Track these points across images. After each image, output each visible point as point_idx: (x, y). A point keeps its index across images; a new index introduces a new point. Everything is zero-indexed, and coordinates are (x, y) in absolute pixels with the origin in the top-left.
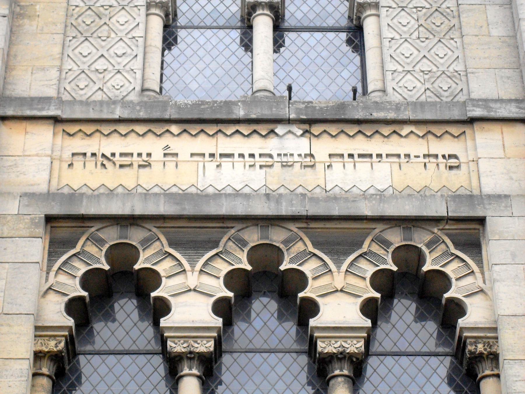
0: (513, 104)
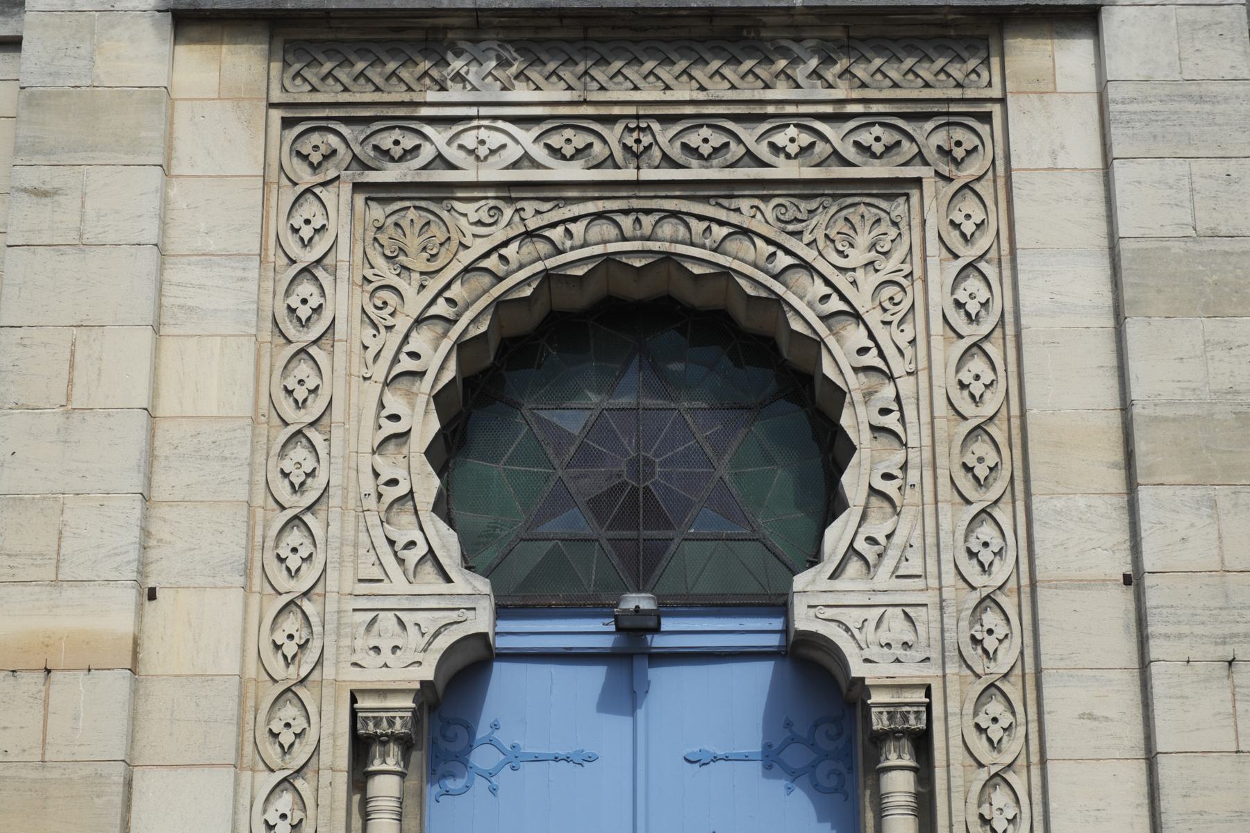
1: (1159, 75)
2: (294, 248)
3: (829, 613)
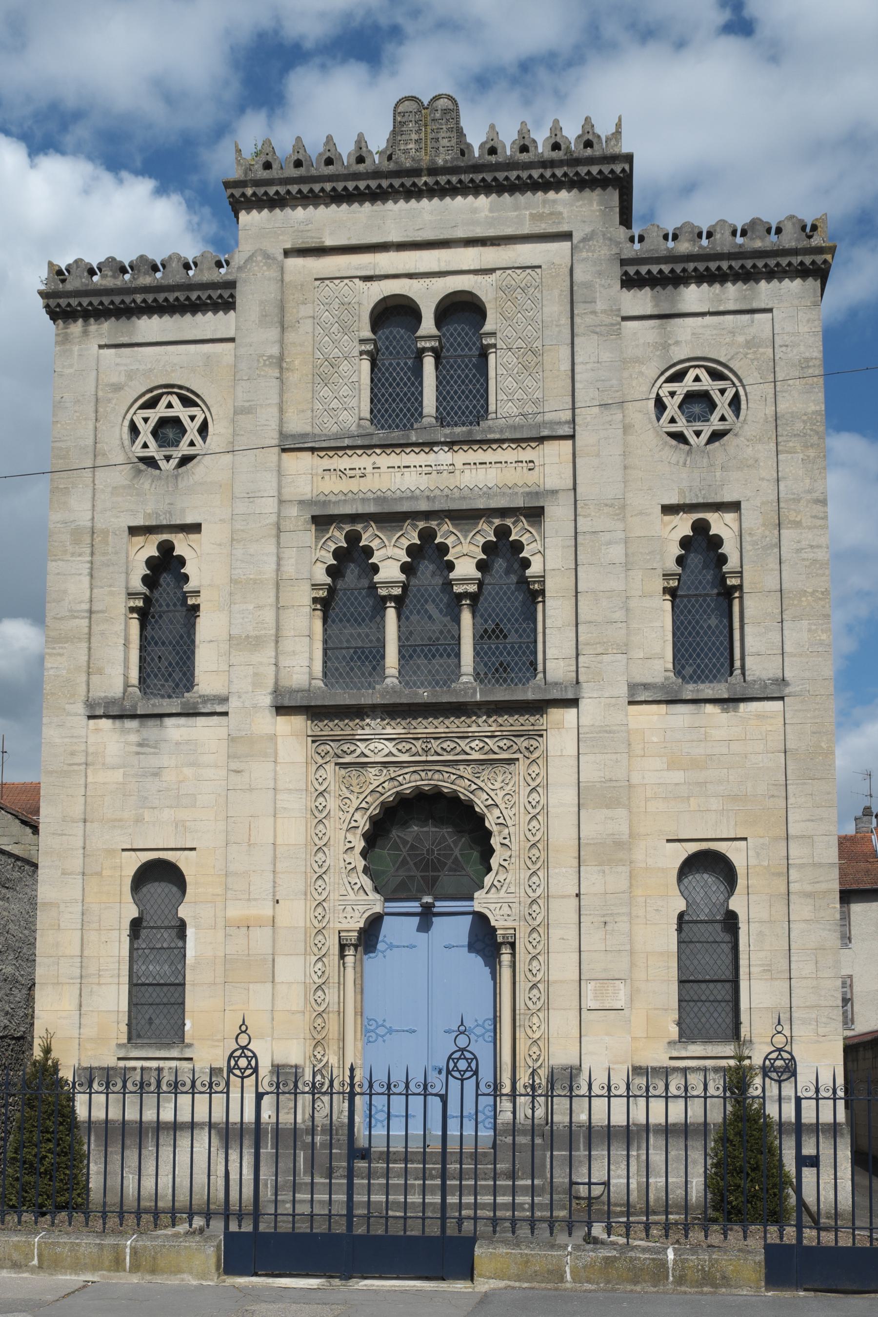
0: (567, 425)
1: (597, 724)
2: (317, 786)
3: (485, 905)
